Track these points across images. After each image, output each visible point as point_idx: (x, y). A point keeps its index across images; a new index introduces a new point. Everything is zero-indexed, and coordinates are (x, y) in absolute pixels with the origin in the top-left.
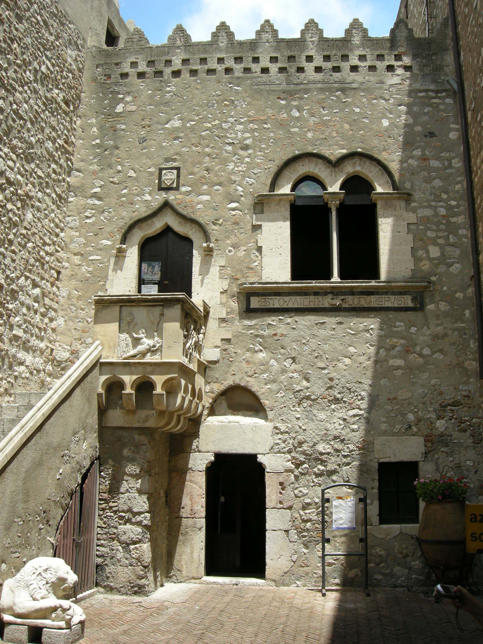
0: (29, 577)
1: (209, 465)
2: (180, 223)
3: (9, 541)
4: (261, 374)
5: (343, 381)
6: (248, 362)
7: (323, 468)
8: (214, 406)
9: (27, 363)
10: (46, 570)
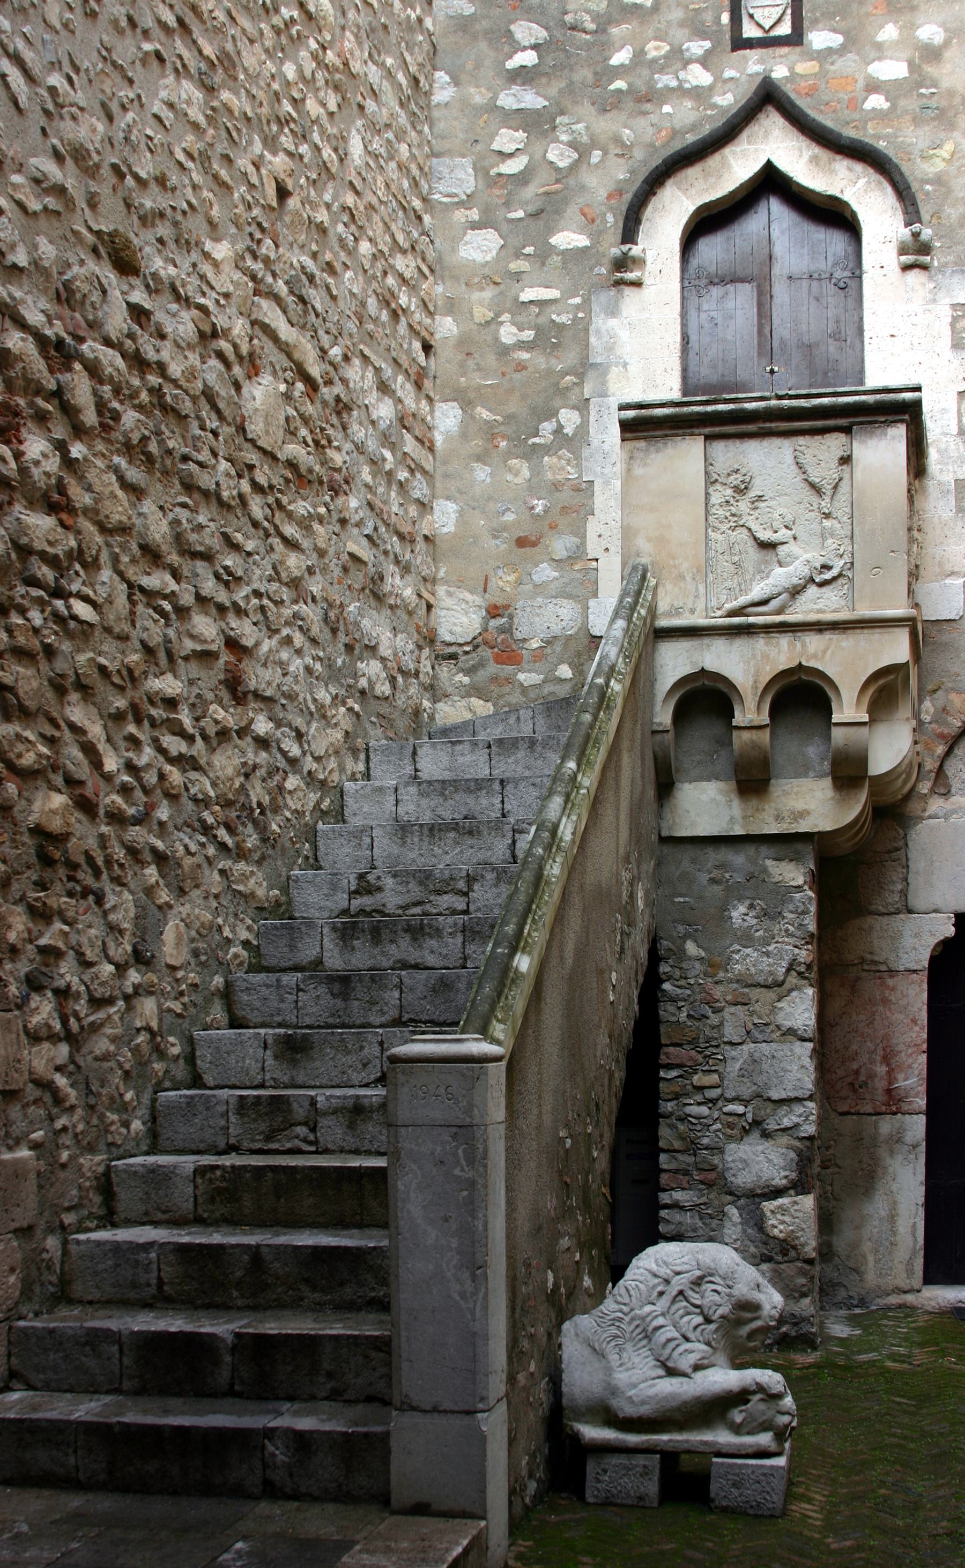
2: (814, 160)
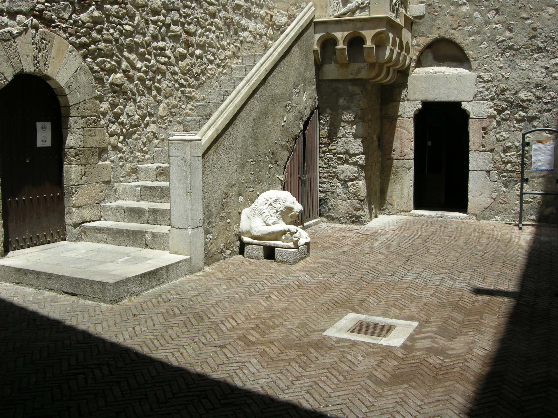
0: (262, 207)
1: (417, 113)
3: (244, 177)
4: (466, 26)
5: (546, 30)
6: (452, 16)
7: (524, 114)
8: (421, 58)
9: (250, 29)
10: (275, 201)
